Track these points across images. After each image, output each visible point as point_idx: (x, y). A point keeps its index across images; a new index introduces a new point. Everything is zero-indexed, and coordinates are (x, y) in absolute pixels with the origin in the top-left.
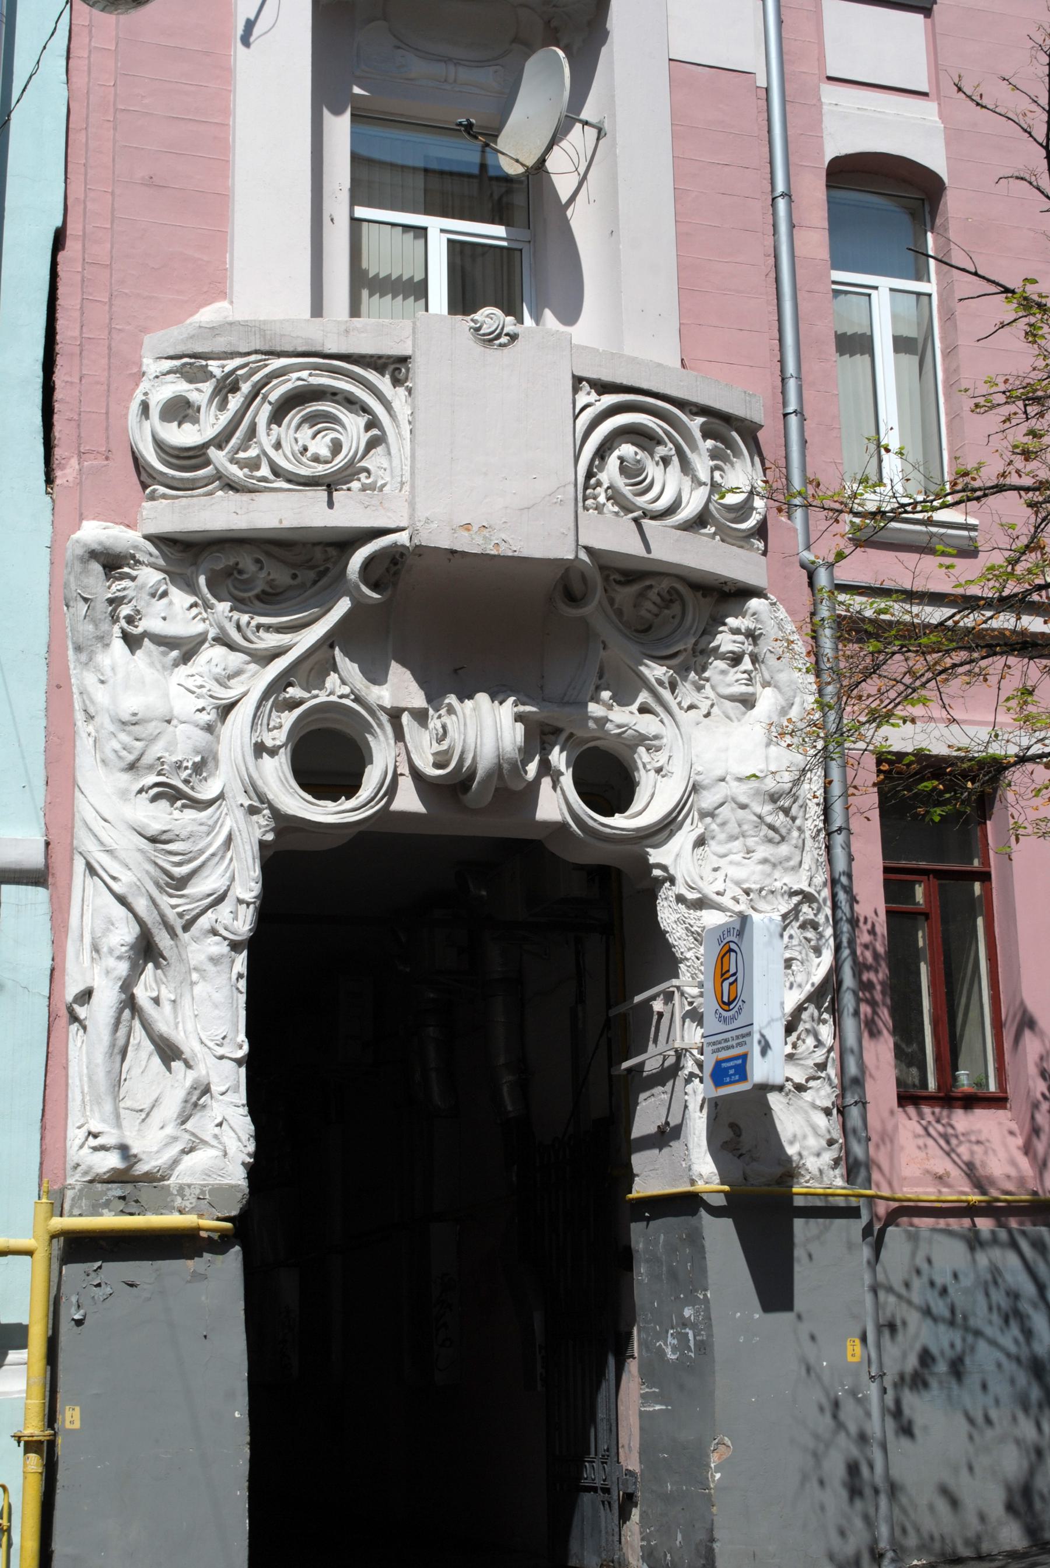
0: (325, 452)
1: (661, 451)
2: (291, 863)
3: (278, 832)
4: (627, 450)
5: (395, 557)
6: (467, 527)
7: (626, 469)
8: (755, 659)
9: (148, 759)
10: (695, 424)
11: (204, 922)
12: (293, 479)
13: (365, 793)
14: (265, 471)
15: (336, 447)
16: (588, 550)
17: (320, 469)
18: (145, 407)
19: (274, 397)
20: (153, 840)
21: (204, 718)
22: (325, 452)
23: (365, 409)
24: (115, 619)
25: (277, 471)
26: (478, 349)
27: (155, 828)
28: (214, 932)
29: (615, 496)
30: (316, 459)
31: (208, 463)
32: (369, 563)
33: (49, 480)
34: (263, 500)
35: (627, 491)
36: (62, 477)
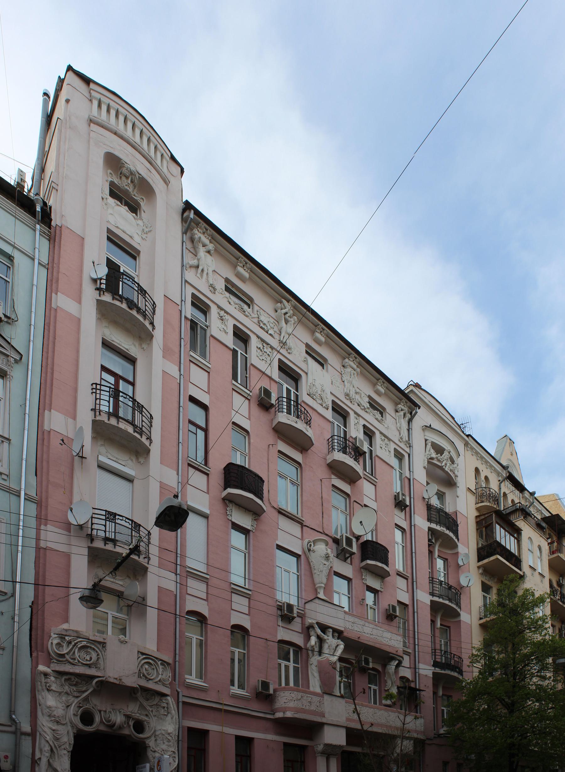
0: (88, 659)
2: (79, 737)
3: (77, 731)
5: (102, 682)
6: (116, 679)
7: (146, 670)
8: (167, 708)
9: (53, 714)
11: (63, 747)
12: (82, 663)
13: (94, 726)
14: (76, 661)
15: (91, 658)
16: (139, 685)
17: (88, 662)
18: (52, 643)
19: (79, 646)
20: (54, 730)
21: (63, 708)
22: (88, 659)
23: (97, 652)
24: (46, 686)
25: (79, 661)
26: (119, 644)
27: (54, 728)
28: (65, 749)
30: (87, 660)
31: (65, 657)
32: (97, 682)
33: (31, 655)
34: (77, 667)
35: (146, 674)
36: (34, 654)
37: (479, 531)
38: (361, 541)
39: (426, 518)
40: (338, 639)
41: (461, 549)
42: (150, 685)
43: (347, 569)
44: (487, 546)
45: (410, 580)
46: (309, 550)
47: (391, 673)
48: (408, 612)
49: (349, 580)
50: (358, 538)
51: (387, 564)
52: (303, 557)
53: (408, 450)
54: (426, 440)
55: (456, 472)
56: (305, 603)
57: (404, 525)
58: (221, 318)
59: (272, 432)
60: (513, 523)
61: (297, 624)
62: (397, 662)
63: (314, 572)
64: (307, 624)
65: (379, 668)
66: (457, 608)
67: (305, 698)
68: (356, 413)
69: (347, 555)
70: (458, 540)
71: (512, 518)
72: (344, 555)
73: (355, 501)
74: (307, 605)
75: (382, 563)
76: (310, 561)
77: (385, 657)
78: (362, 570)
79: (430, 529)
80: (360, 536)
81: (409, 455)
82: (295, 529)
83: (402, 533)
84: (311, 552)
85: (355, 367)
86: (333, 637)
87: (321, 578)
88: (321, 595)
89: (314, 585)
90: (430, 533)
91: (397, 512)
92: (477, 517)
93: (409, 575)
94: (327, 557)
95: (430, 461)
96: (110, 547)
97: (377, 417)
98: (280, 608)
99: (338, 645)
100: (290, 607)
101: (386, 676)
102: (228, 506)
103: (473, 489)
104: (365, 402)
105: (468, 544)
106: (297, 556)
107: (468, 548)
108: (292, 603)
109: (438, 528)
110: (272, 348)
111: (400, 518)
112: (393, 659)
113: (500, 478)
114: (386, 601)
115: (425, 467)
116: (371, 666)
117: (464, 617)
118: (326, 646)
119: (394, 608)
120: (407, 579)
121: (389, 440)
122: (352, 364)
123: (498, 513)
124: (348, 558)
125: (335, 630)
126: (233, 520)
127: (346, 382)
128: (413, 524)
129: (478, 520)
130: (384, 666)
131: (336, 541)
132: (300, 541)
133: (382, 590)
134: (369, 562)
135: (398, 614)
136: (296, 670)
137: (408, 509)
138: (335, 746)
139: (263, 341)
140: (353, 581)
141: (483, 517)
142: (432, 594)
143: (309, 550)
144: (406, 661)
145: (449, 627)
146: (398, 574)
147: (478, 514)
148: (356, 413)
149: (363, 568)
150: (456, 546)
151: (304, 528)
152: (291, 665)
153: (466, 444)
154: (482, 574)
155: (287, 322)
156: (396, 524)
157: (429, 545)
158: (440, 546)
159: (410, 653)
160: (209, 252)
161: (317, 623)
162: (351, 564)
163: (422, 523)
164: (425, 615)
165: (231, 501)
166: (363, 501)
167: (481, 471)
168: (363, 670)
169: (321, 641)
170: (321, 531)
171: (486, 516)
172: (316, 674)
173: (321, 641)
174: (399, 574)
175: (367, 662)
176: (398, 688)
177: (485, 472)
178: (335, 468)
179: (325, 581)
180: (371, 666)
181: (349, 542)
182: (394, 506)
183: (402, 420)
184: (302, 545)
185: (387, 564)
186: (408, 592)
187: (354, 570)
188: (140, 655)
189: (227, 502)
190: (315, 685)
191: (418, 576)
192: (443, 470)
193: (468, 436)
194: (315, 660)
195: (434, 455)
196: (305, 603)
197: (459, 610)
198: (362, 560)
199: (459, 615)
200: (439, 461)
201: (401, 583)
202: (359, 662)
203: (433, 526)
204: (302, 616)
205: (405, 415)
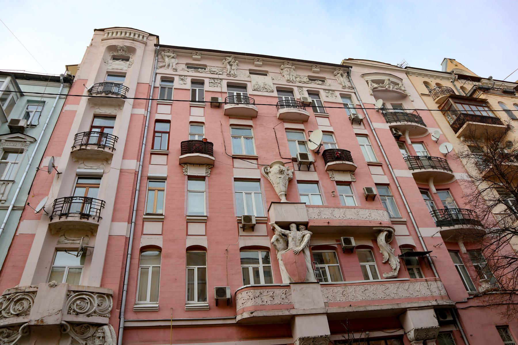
1: (87, 301)
4: (78, 302)
10: (95, 297)
29: (74, 311)
39: (385, 121)
42: (82, 319)
44: (457, 120)
47: (383, 245)
53: (353, 91)
54: (367, 81)
55: (403, 88)
58: (182, 80)
59: (224, 117)
67: (265, 293)
68: (298, 87)
77: (372, 233)
79: (391, 128)
81: (355, 93)
85: (291, 66)
86: (298, 229)
90: (393, 129)
91: (355, 126)
94: (281, 172)
95: (374, 90)
96: (63, 219)
97: (318, 83)
99: (304, 236)
100: (248, 219)
103: (427, 92)
104: (306, 79)
110: (221, 79)
112: (380, 231)
113: (451, 80)
115: (371, 95)
118: (290, 239)
120: (381, 166)
121: (334, 91)
122: (288, 66)
125: (298, 225)
127: (285, 76)
128: (372, 129)
130: (375, 241)
131: (294, 160)
137: (365, 121)
138: (314, 338)
139: (214, 79)
143: (267, 173)
144: (400, 230)
146: (368, 165)
148: (298, 87)
153: (407, 73)
154: (465, 141)
155: (231, 65)
156: (356, 134)
158: (409, 136)
159: (406, 221)
160: (173, 58)
161: (277, 223)
163: (382, 126)
165: (186, 164)
167: (430, 82)
174: (370, 164)
177: (433, 82)
178: (283, 119)
180: (354, 243)
183: (341, 78)
186: (385, 174)
188: (72, 293)
192: (390, 91)
193: (406, 68)
195: (375, 85)
200: (382, 87)
205: (342, 75)
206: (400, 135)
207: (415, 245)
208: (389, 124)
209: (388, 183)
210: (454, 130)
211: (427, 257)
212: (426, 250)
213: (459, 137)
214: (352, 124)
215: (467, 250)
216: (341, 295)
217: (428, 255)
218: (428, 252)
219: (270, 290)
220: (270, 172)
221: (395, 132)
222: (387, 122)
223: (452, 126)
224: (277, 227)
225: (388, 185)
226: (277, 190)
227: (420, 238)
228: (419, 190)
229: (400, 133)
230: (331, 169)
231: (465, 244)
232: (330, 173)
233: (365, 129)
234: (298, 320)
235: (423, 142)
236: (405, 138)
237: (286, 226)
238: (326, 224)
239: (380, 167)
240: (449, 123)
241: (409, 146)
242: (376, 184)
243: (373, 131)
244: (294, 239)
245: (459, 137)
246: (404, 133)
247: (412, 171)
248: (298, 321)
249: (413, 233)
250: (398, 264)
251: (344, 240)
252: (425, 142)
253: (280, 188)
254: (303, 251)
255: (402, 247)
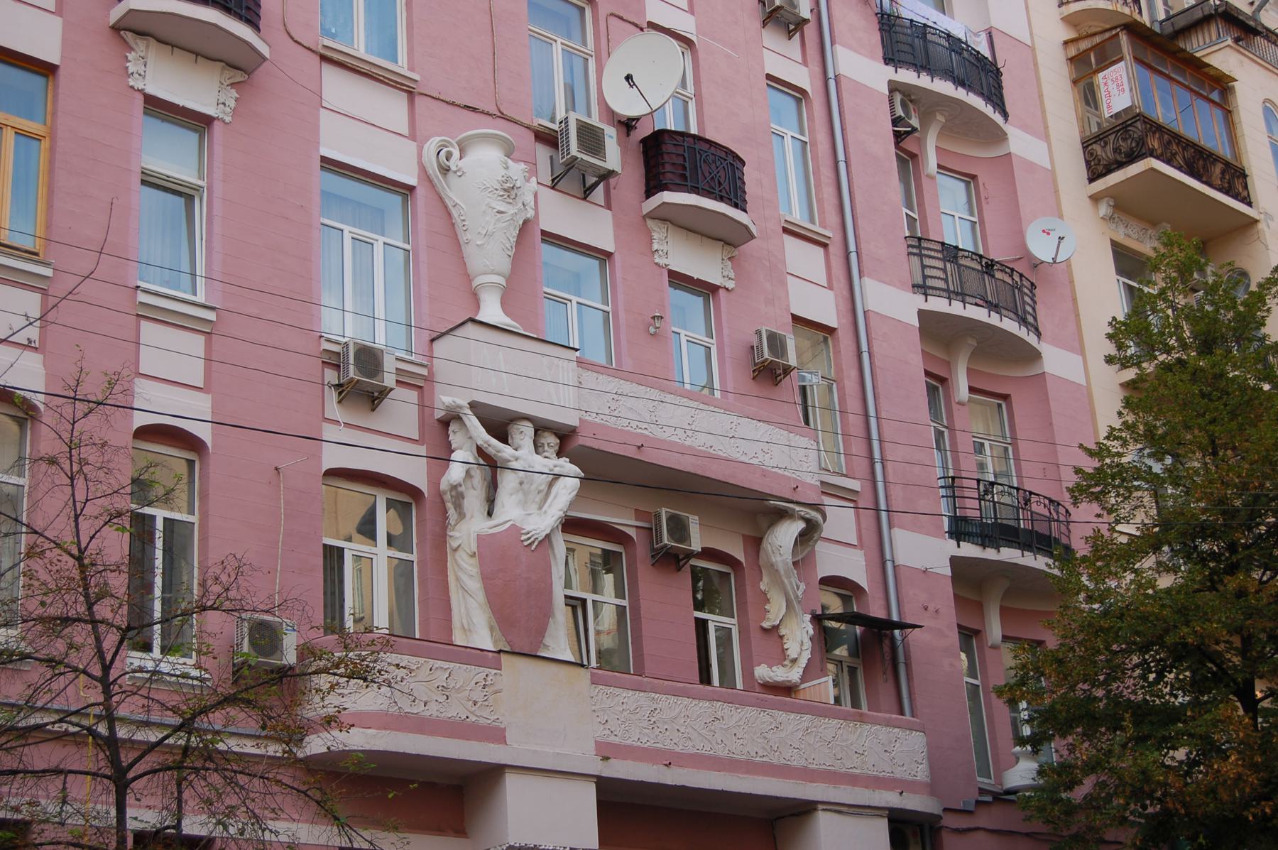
37: (1081, 85)
38: (644, 131)
40: (559, 454)
41: (1020, 143)
43: (592, 224)
45: (835, 249)
46: (445, 170)
48: (837, 352)
49: (604, 257)
50: (627, 125)
51: (738, 201)
52: (421, 193)
56: (432, 340)
57: (802, 77)
60: (1198, 59)
61: (402, 412)
62: (801, 525)
63: (463, 238)
64: (439, 414)
65: (740, 555)
66: (1022, 333)
67: (423, 674)
69: (591, 180)
70: (1005, 115)
71: (1198, 46)
72: (580, 181)
73: (612, 14)
74: (436, 344)
75: (721, 199)
76: (450, 204)
77: (756, 510)
78: (650, 223)
79: (894, 87)
80: (637, 119)
82: (393, 109)
83: (798, 101)
84: (450, 174)
86: (537, 448)
87: (489, 255)
88: (492, 311)
89: (468, 279)
90: (898, 98)
91: (771, 38)
92: (1066, 43)
93: (830, 233)
98: (334, 361)
100: (369, 358)
101: (765, 579)
102: (131, 49)
105: (1045, 133)
106: (406, 191)
107: (1047, 138)
108: (380, 341)
109: (924, 81)
111: (783, 58)
112: (781, 515)
114: (752, 318)
116: (696, 545)
117: (1057, 361)
118: (507, 481)
119: (776, 342)
120: (825, 246)
123: (1134, 29)
124: (595, 185)
125: (541, 427)
126: (152, 90)
128: (831, 75)
129: (1073, 52)
130: (755, 543)
131: (548, 138)
132: (412, 146)
133: (731, 285)
134: (668, 197)
135: (792, 361)
136: (402, 573)
137: (810, 30)
140: (617, 257)
141: (1084, 45)
142: (922, 289)
144: (840, 521)
145: (1006, 397)
146: (785, 230)
147: (1071, 35)
149: (652, 215)
150: (1001, 137)
151: (418, 100)
152: (381, 553)
156: (769, 77)
157: (898, 137)
161: (473, 406)
162: (608, 206)
163: (864, 70)
164: (904, 361)
165: (140, 34)
166: (642, 11)
168: (670, 560)
169: (492, 465)
170: (493, 110)
171: (1098, 39)
172: (475, 585)
173: (492, 465)
175: (679, 528)
176: (817, 619)
179: (505, 264)
181: (591, 139)
182: (758, 24)
184: (420, 156)
185: (738, 201)
186: (830, 287)
187: (617, 225)
189: (129, 36)
190: (475, 624)
191: (861, 234)
194: (470, 529)
196: (432, 340)
197: (1031, 339)
198: (649, 193)
199: (1034, 356)
201: (804, 261)
202: (651, 532)
203: (907, 76)
204: (421, 384)
206: (914, 130)
207: (863, 583)
208: (889, 73)
209: (834, 324)
210: (1088, 163)
211: (893, 638)
212: (895, 618)
213: (1095, 198)
214: (764, 24)
215: (1004, 637)
216: (645, 724)
217: (897, 632)
218: (902, 626)
219: (439, 663)
220: (460, 173)
221: (900, 112)
222: (888, 60)
223: (1086, 144)
224: (473, 423)
225: (831, 331)
226: (476, 260)
227: (889, 565)
228: (923, 378)
229: (914, 122)
230: (666, 216)
231: (1005, 612)
232: (659, 233)
233: (805, 62)
234: (512, 782)
235: (974, 177)
236: (921, 142)
237: (500, 425)
238: (631, 452)
239: (820, 250)
240: (1081, 132)
241: (924, 180)
242: (796, 319)
243: (832, 84)
244: (525, 486)
245: (1095, 198)
246: (926, 118)
247: (918, 301)
248: (514, 788)
249: (870, 539)
250: (808, 644)
251: (673, 519)
252: (981, 180)
253: (489, 255)
254: (548, 536)
255: (831, 582)
